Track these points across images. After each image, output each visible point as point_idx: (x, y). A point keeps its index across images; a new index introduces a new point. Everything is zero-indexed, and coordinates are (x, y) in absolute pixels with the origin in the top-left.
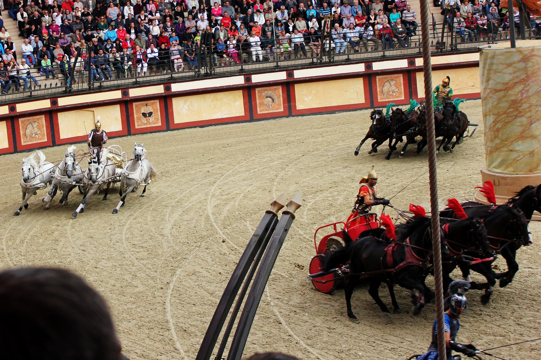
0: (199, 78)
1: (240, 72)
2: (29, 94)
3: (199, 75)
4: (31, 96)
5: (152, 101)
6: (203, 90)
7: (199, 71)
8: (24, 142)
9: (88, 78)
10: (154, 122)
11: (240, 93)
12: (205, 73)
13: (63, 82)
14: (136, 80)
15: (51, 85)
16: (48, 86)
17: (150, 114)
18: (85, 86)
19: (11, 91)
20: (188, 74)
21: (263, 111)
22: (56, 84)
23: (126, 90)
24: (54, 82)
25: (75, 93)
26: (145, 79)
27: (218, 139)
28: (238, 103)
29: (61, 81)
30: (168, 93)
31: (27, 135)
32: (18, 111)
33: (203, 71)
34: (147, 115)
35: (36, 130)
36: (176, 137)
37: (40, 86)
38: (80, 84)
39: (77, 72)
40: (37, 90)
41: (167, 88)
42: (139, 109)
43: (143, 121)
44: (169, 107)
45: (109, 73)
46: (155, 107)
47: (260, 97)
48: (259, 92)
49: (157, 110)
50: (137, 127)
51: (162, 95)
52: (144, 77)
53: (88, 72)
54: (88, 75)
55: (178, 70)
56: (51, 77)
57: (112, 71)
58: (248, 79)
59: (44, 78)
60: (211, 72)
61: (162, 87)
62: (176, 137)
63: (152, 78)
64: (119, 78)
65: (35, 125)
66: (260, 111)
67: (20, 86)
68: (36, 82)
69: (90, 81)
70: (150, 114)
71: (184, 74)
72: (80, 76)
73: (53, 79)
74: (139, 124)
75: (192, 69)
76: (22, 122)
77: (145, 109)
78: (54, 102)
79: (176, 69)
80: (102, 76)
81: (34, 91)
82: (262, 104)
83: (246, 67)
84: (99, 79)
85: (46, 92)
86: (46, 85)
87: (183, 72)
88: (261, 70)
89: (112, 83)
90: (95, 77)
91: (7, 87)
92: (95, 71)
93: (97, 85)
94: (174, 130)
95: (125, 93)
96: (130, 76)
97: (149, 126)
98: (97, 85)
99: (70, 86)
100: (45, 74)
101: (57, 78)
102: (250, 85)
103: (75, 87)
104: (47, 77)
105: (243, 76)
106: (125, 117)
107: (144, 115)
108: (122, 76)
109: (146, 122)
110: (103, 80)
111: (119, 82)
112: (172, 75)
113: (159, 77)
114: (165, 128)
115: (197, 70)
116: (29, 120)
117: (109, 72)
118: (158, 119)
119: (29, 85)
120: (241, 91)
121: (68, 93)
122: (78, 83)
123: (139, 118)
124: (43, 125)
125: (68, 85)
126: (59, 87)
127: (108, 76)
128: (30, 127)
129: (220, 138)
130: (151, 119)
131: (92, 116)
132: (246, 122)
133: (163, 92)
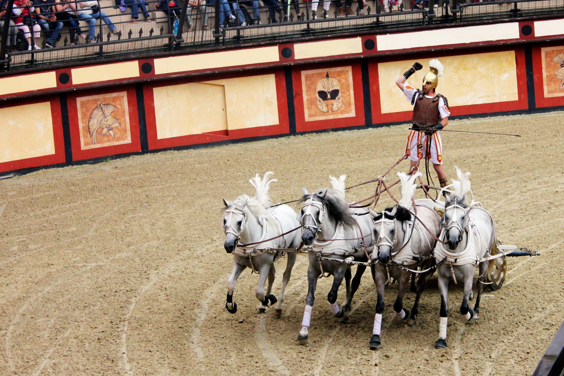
0: (431, 26)
1: (511, 16)
2: (97, 49)
3: (430, 19)
4: (100, 53)
5: (339, 69)
6: (439, 49)
7: (432, 11)
8: (86, 144)
9: (213, 22)
10: (342, 108)
11: (510, 57)
12: (442, 16)
13: (165, 26)
14: (308, 26)
15: (141, 32)
16: (135, 35)
17: (335, 94)
18: (209, 36)
19: (61, 43)
20: (409, 17)
21: (555, 92)
22: (152, 31)
23: (288, 46)
24: (146, 27)
25: (188, 50)
26: (325, 25)
27: (467, 147)
28: (505, 76)
29: (160, 25)
30: (371, 54)
31: (92, 130)
32: (74, 83)
33: (438, 11)
34: (329, 96)
35: (110, 120)
36: (384, 140)
37: (119, 34)
38: (197, 32)
39: (193, 7)
40: (114, 43)
41: (370, 44)
42: (312, 84)
43: (320, 107)
44: (371, 80)
45: (254, 12)
46: (344, 81)
47: (548, 65)
48: (547, 54)
49: (348, 86)
50: (307, 119)
51: (358, 56)
52: (325, 20)
53: (213, 10)
54: (214, 15)
55: (390, 8)
56: (141, 16)
57: (260, 7)
58: (527, 30)
59: (127, 18)
60: (455, 14)
61: (358, 41)
62: (384, 140)
63: (339, 24)
64: (274, 21)
65: (108, 110)
66: (550, 92)
67: (80, 32)
68: (110, 25)
69: (217, 26)
70: (335, 94)
71: (402, 17)
72: (199, 16)
73: (145, 20)
74: (313, 112)
75: (417, 8)
76: (82, 104)
77: (324, 85)
78: (147, 68)
79: (386, 7)
80: (242, 18)
81: (108, 43)
82: (552, 79)
83: (523, 6)
84: (236, 24)
85: (131, 46)
86: (130, 33)
87: (400, 12)
88: (552, 11)
89: (261, 31)
90: (227, 18)
91: (55, 35)
92: (228, 7)
93: (231, 34)
94: (381, 125)
95: (286, 53)
96: (295, 19)
97: (331, 117)
98: (231, 34)
99: (179, 36)
100: (129, 10)
101: (154, 19)
102: (531, 40)
103: (188, 37)
104: (135, 17)
105: (516, 25)
106: (285, 100)
107: (323, 95)
108: (280, 18)
109: (325, 109)
110: (244, 24)
111: (275, 30)
112: (378, 19)
113: (353, 22)
114: (363, 122)
115: (427, 9)
116: (96, 100)
117: (254, 10)
118: (350, 104)
119: (97, 31)
120: (513, 53)
121: (175, 49)
122: (195, 30)
123: (312, 102)
124: (124, 112)
125: (175, 33)
126: (156, 38)
127: (252, 16)
128: (98, 114)
129: (469, 144)
130: (335, 104)
131: (220, 95)
132: (520, 112)
133: (361, 51)
